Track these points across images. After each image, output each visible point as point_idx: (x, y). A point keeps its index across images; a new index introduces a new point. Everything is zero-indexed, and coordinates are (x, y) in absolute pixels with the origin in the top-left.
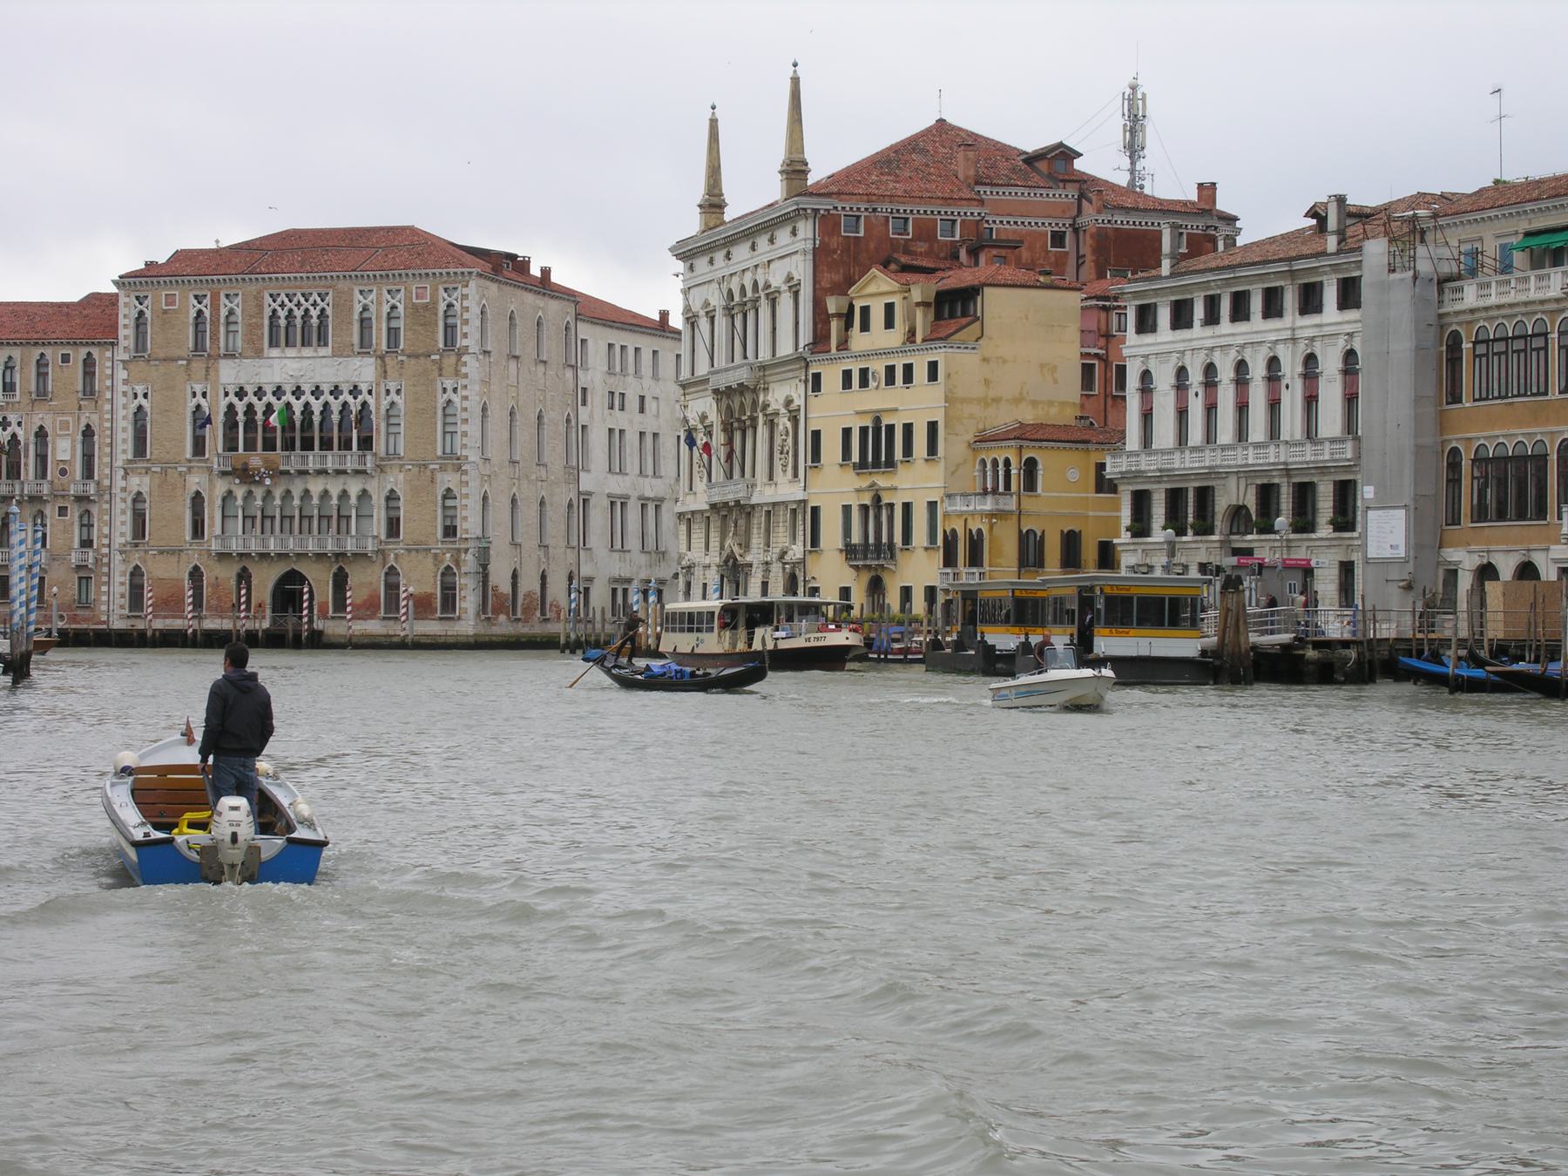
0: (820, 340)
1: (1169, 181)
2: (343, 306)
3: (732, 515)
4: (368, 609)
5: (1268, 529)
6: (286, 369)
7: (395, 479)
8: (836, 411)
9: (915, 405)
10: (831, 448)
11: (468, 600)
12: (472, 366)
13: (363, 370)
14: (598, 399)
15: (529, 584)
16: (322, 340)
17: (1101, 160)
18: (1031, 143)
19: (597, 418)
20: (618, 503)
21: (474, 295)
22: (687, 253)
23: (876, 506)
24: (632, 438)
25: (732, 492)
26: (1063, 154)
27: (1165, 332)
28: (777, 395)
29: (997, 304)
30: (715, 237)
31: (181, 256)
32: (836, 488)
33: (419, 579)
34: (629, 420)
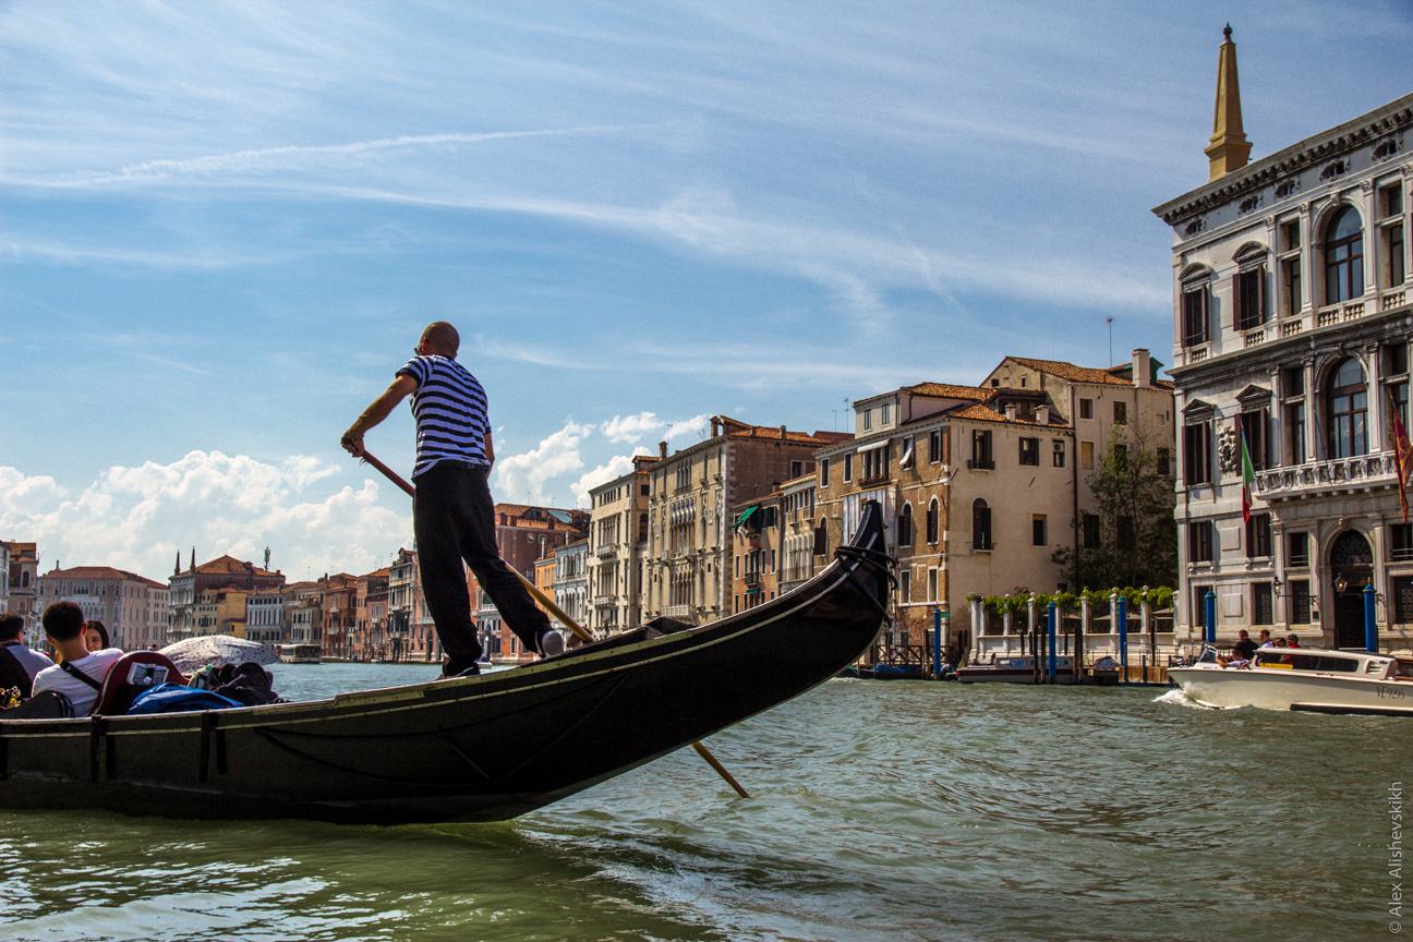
0: (195, 602)
1: (272, 569)
5: (267, 639)
8: (198, 615)
9: (212, 615)
10: (197, 622)
12: (123, 599)
13: (96, 600)
14: (152, 605)
16: (87, 592)
17: (259, 564)
18: (244, 561)
19: (152, 611)
21: (126, 583)
24: (160, 614)
27: (254, 606)
30: (178, 576)
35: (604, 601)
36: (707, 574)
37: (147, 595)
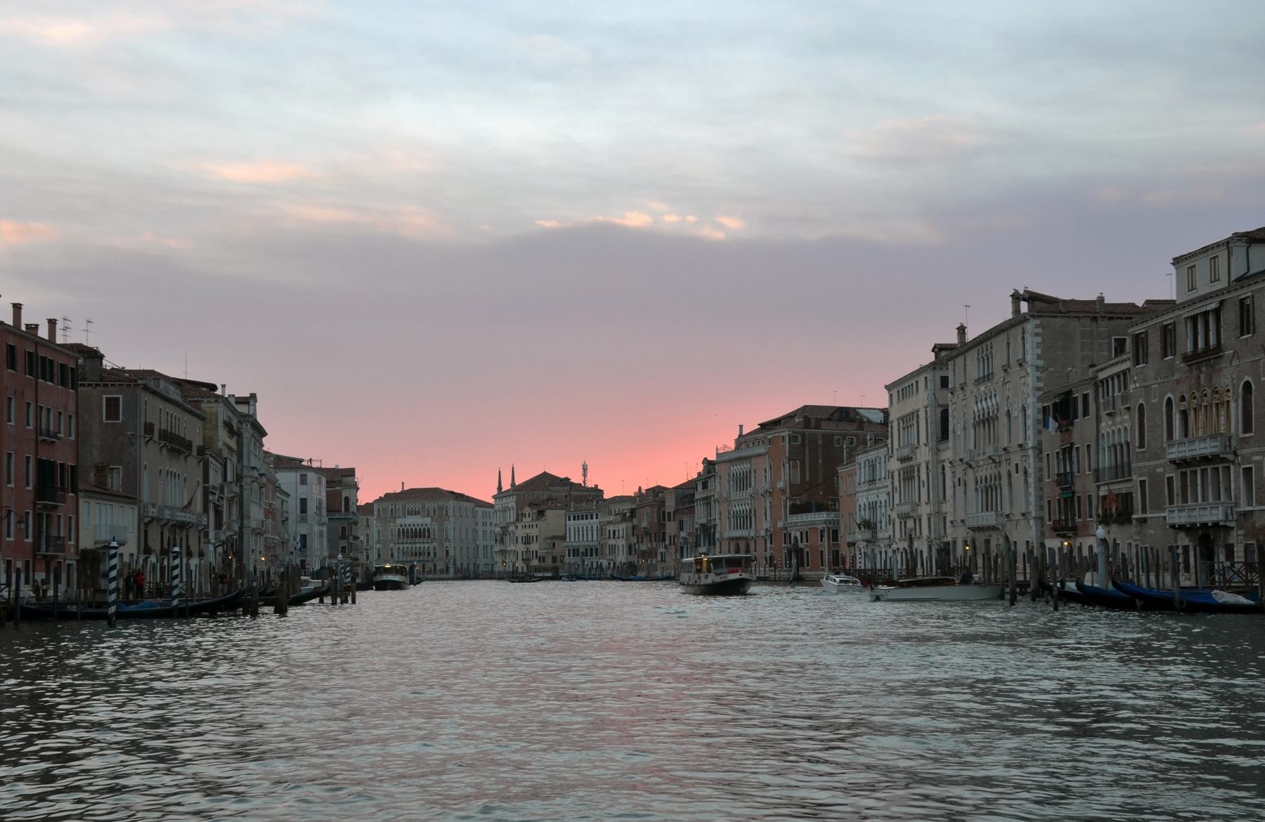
1: (590, 485)
2: (423, 506)
3: (503, 552)
4: (429, 572)
6: (411, 520)
7: (435, 544)
8: (521, 533)
9: (534, 532)
11: (451, 570)
12: (451, 519)
13: (428, 520)
15: (465, 566)
17: (576, 479)
18: (562, 476)
19: (480, 529)
20: (485, 547)
21: (452, 504)
22: (494, 497)
23: (528, 551)
25: (503, 548)
26: (567, 479)
28: (512, 528)
29: (549, 513)
30: (501, 494)
31: (386, 495)
32: (521, 548)
33: (440, 566)
34: (488, 528)
35: (906, 509)
36: (1014, 474)
37: (475, 516)
